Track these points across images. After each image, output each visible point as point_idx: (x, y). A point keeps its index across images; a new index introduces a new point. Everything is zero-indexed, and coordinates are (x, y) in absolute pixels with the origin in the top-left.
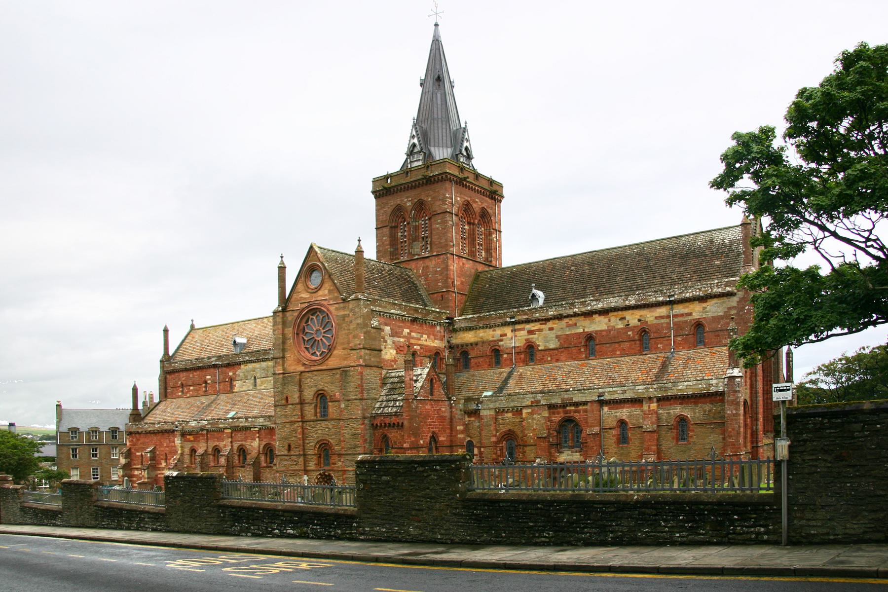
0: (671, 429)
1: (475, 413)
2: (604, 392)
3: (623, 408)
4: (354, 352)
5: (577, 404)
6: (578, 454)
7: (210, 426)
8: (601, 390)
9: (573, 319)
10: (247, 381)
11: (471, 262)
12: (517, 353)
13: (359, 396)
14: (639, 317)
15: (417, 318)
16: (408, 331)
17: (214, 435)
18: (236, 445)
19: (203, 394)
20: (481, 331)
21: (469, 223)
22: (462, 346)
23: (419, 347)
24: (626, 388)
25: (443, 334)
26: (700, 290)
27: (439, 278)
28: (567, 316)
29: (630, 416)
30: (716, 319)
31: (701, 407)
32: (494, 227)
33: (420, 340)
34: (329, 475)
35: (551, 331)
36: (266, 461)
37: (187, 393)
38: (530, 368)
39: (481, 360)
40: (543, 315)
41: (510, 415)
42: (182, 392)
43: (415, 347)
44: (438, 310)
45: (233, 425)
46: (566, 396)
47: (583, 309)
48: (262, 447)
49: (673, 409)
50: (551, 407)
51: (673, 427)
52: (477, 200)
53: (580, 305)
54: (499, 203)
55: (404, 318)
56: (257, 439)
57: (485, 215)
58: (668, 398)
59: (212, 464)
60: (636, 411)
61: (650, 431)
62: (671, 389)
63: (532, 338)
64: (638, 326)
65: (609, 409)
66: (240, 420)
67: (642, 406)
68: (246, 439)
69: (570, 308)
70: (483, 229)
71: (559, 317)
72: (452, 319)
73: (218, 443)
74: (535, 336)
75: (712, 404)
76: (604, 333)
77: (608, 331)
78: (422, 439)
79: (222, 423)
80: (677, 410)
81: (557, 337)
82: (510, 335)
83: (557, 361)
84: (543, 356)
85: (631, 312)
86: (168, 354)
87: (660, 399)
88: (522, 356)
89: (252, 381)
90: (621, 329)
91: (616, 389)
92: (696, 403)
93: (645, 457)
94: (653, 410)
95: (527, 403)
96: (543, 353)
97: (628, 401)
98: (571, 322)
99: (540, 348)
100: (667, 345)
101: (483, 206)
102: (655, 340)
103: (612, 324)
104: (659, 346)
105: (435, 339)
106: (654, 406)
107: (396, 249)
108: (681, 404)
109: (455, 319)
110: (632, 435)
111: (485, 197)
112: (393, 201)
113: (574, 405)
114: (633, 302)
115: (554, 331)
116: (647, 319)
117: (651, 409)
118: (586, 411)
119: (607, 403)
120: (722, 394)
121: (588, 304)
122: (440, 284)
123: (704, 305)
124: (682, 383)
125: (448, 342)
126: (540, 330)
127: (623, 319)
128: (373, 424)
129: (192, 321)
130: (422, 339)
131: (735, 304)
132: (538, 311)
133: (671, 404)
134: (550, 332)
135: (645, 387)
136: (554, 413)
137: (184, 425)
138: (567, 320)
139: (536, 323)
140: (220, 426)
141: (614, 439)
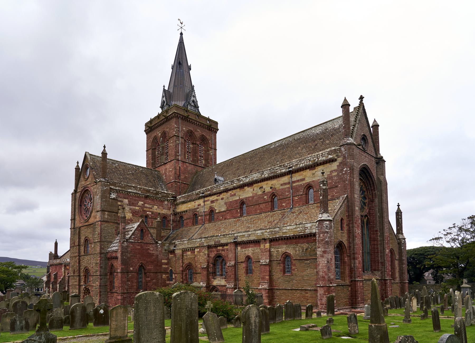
0: (279, 264)
1: (173, 252)
2: (238, 236)
3: (249, 247)
4: (98, 212)
5: (223, 245)
6: (224, 280)
8: (236, 235)
9: (234, 191)
11: (193, 165)
12: (205, 215)
13: (99, 240)
14: (270, 186)
15: (148, 196)
16: (143, 203)
20: (189, 203)
21: (193, 144)
22: (180, 213)
23: (150, 213)
24: (250, 233)
25: (169, 206)
27: (171, 174)
28: (231, 190)
29: (253, 254)
31: (300, 246)
32: (211, 147)
33: (151, 208)
34: (88, 288)
35: (223, 200)
38: (210, 224)
39: (188, 221)
41: (189, 253)
43: (148, 213)
44: (166, 192)
46: (217, 240)
47: (239, 184)
49: (280, 248)
50: (209, 247)
51: (281, 262)
52: (198, 130)
53: (237, 181)
54: (215, 133)
55: (139, 195)
57: (205, 140)
58: (276, 239)
60: (257, 250)
61: (264, 265)
63: (213, 205)
64: (270, 192)
65: (241, 248)
67: (260, 246)
69: (232, 184)
70: (203, 148)
71: (226, 191)
72: (176, 197)
74: (214, 204)
75: (308, 243)
76: (250, 199)
77: (253, 197)
78: (132, 267)
80: (283, 249)
82: (202, 204)
83: (225, 219)
84: (218, 216)
85: (266, 182)
87: (271, 240)
88: (208, 217)
90: (261, 195)
91: (244, 234)
92: (297, 243)
93: (261, 285)
94: (267, 248)
95: (197, 245)
96: (218, 214)
97: (252, 242)
98: (232, 194)
99: (217, 211)
100: (288, 203)
101: (203, 134)
102: (280, 200)
103: (255, 192)
104: (283, 204)
105: (164, 209)
106: (267, 245)
107: (155, 161)
108: (286, 244)
109: (177, 197)
110: (255, 267)
111: (204, 129)
112: (153, 134)
113: (221, 246)
114: (266, 176)
116: (276, 187)
117: (266, 248)
118: (227, 250)
119: (239, 244)
120: (314, 235)
121: (241, 180)
122: (171, 178)
124: (285, 228)
125: (174, 211)
126: (217, 200)
127: (261, 188)
128: (107, 257)
130: (153, 208)
132: (215, 188)
133: (279, 244)
134: (221, 201)
135: (261, 231)
136: (211, 251)
138: (230, 192)
139: (215, 196)
141: (244, 270)
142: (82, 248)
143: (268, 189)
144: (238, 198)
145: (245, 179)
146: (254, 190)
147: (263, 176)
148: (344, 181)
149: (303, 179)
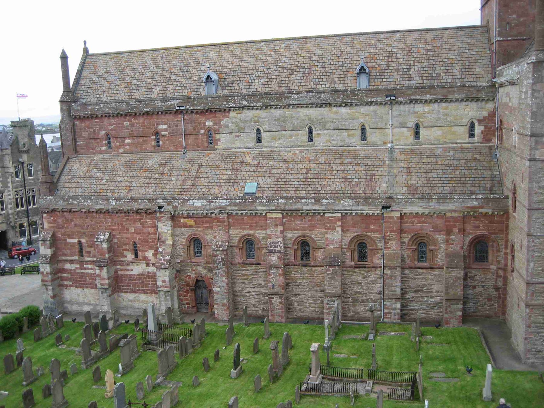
7: (235, 208)
10: (242, 135)
17: (243, 220)
18: (291, 236)
19: (153, 149)
36: (353, 259)
37: (118, 148)
42: (109, 145)
45: (287, 208)
48: (347, 240)
56: (339, 229)
59: (238, 260)
66: (303, 201)
68: (312, 228)
73: (251, 232)
79: (261, 204)
89: (254, 135)
129: (85, 42)
137: (176, 204)
140: (258, 208)
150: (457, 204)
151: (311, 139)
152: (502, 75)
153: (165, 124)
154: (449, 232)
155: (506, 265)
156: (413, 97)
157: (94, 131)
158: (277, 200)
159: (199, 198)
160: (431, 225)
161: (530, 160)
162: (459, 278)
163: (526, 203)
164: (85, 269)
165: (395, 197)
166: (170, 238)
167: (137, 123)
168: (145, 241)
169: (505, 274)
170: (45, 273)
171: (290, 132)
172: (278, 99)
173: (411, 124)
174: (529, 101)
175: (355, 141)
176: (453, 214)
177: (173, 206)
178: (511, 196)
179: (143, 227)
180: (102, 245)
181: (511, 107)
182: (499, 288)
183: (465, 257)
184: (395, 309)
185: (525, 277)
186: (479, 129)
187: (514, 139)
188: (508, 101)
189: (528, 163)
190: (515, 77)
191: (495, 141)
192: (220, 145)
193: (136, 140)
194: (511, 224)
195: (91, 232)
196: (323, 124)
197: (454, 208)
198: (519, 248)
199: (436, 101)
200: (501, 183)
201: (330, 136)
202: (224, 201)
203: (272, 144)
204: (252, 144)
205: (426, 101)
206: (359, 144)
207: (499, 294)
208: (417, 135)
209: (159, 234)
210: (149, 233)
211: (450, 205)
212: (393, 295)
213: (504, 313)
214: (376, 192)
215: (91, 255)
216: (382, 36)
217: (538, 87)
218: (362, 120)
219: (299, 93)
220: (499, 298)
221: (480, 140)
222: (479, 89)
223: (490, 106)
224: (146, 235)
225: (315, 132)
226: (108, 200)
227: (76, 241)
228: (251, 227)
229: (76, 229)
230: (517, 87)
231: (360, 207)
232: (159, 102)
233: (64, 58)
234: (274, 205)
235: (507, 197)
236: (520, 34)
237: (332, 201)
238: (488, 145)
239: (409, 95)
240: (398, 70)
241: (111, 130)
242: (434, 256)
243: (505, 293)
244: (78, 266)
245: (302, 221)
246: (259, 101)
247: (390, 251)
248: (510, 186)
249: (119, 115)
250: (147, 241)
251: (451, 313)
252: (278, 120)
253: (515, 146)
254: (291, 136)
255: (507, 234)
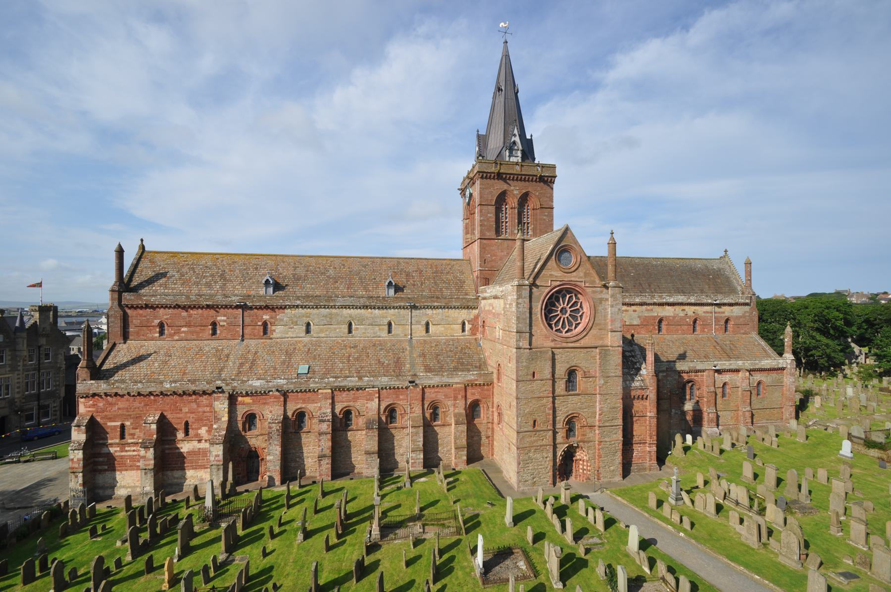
2: (718, 364)
8: (715, 363)
14: (693, 310)
24: (731, 362)
26: (732, 299)
30: (738, 318)
37: (171, 335)
40: (632, 301)
42: (162, 333)
45: (336, 385)
46: (692, 365)
62: (757, 364)
68: (355, 399)
71: (642, 304)
73: (303, 406)
76: (671, 318)
77: (674, 317)
80: (758, 377)
81: (639, 317)
85: (688, 307)
86: (124, 282)
114: (693, 301)
115: (636, 313)
120: (783, 369)
123: (732, 308)
126: (626, 311)
129: (142, 240)
131: (748, 310)
137: (236, 384)
138: (644, 307)
140: (312, 385)
142: (561, 386)
143: (690, 313)
144: (656, 315)
145: (668, 298)
146: (675, 310)
147: (689, 300)
148: (753, 321)
149: (724, 313)
150: (460, 378)
151: (350, 331)
152: (486, 292)
153: (224, 316)
154: (455, 398)
155: (493, 420)
156: (425, 304)
157: (148, 319)
158: (328, 378)
159: (258, 379)
160: (443, 394)
161: (517, 349)
162: (464, 432)
163: (514, 377)
164: (127, 451)
165: (418, 374)
166: (227, 415)
167: (195, 314)
168: (199, 420)
169: (492, 426)
170: (75, 460)
171: (335, 326)
172: (326, 301)
173: (424, 323)
174: (514, 309)
175: (384, 333)
176: (458, 385)
177: (232, 387)
178: (495, 371)
179: (198, 407)
180: (151, 426)
181: (494, 313)
182: (489, 437)
183: (467, 416)
184: (419, 459)
185: (515, 427)
186: (468, 327)
187: (499, 333)
188: (491, 308)
189: (515, 350)
190: (499, 294)
191: (479, 336)
192: (275, 335)
193: (192, 329)
194: (496, 390)
195: (139, 414)
196: (361, 321)
197: (458, 381)
198: (508, 408)
199: (441, 308)
200: (485, 363)
201: (366, 329)
202: (282, 380)
203: (320, 335)
204: (303, 334)
205: (434, 307)
206: (387, 335)
207: (489, 441)
208: (427, 330)
209: (215, 412)
210: (204, 412)
211: (457, 379)
212: (417, 448)
213: (493, 455)
214: (402, 371)
215: (136, 437)
216: (402, 260)
217: (520, 301)
218: (389, 319)
219: (343, 297)
220: (489, 443)
221: (469, 334)
222: (469, 300)
223: (475, 312)
224: (201, 414)
225: (354, 326)
226: (161, 383)
227: (119, 424)
228: (304, 401)
229: (120, 412)
230: (502, 301)
231: (392, 383)
232: (219, 297)
233: (120, 252)
234: (325, 383)
235: (492, 373)
236: (493, 267)
237: (372, 378)
238: (474, 337)
239: (423, 302)
240: (414, 285)
241: (167, 319)
242: (445, 416)
243: (493, 441)
244: (118, 449)
245: (347, 394)
246: (311, 302)
247: (414, 415)
248: (495, 366)
249: (178, 307)
250: (202, 420)
251: (459, 458)
252: (326, 316)
253: (499, 339)
254: (335, 329)
255: (493, 398)
